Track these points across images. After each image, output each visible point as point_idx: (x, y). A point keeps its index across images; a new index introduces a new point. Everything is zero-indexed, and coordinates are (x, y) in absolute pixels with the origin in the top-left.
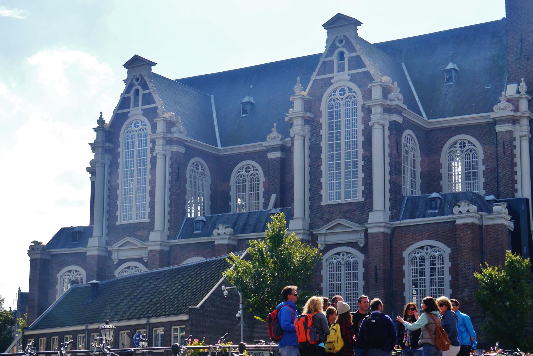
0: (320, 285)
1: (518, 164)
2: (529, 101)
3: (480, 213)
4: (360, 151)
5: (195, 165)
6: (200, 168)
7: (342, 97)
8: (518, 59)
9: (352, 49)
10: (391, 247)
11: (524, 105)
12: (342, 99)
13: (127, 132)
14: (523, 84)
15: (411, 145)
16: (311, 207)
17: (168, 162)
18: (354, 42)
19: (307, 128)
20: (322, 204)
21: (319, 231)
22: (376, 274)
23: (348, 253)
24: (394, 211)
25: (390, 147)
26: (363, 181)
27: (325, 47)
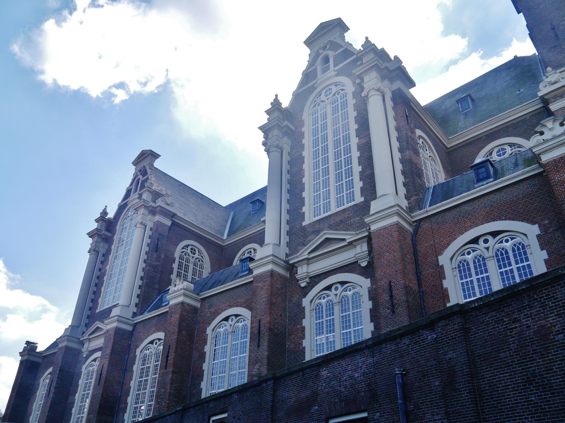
0: (301, 344)
5: (190, 248)
6: (197, 253)
7: (327, 97)
10: (415, 253)
13: (125, 219)
17: (148, 232)
19: (285, 139)
20: (304, 224)
21: (297, 257)
22: (391, 296)
23: (343, 283)
25: (396, 119)
26: (360, 175)
27: (308, 61)
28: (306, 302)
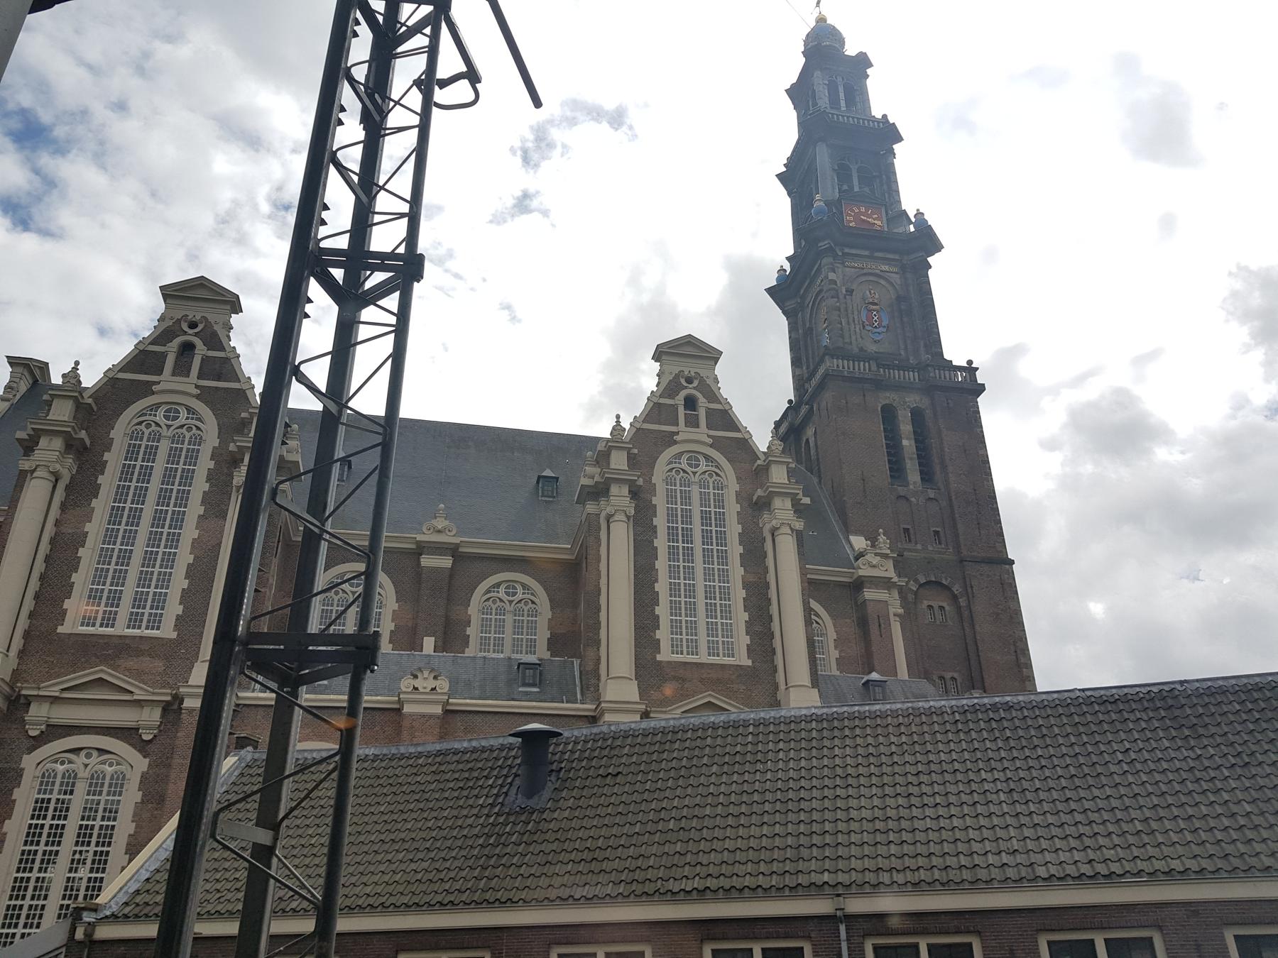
12: (694, 473)
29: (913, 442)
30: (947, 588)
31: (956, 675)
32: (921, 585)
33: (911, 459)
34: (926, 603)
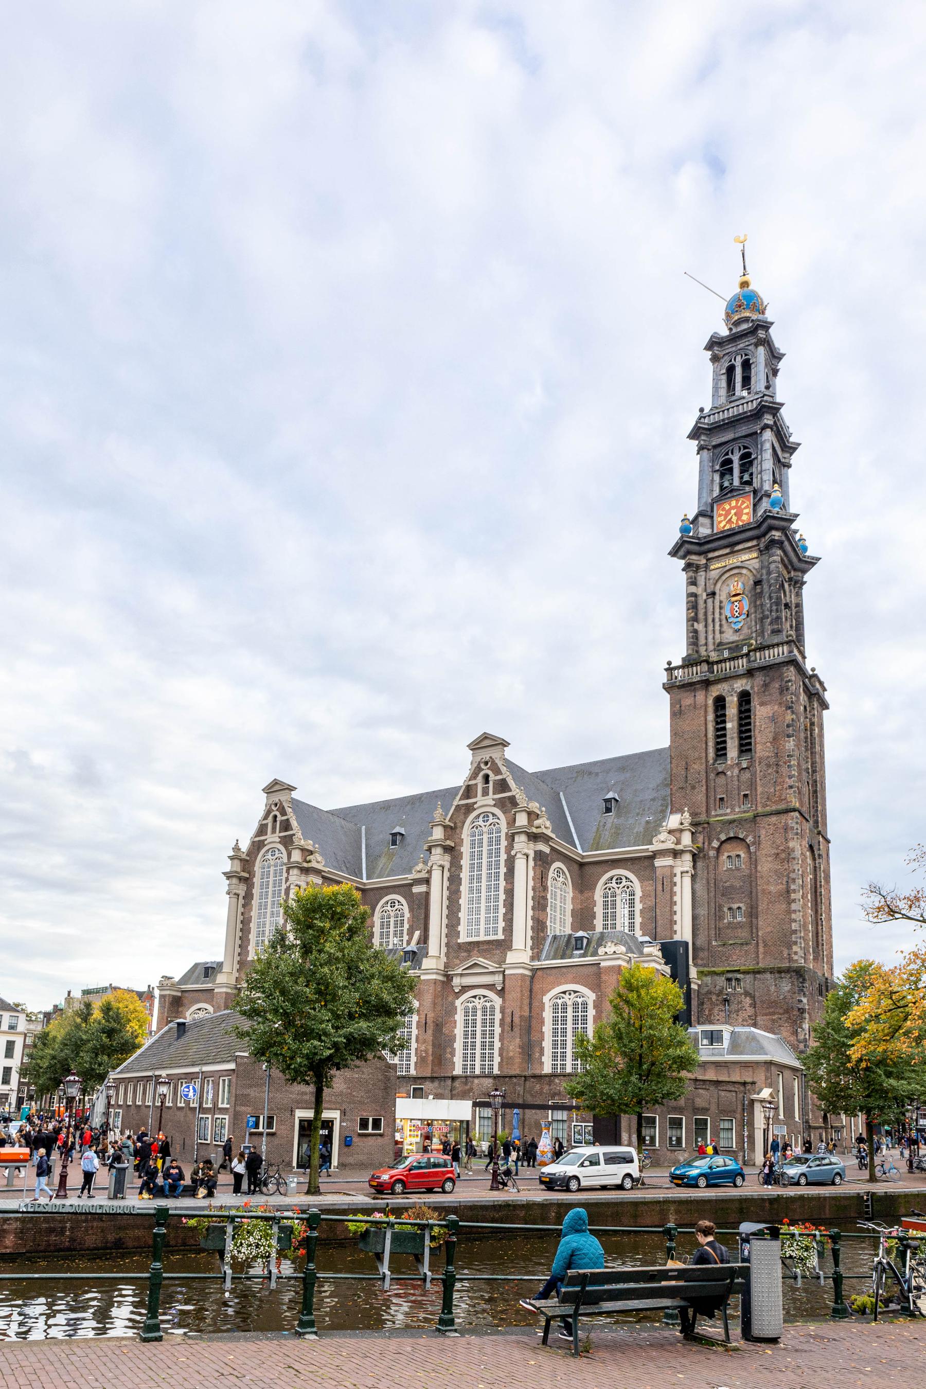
1: (679, 903)
2: (693, 833)
3: (629, 955)
4: (502, 883)
8: (682, 788)
9: (497, 771)
11: (686, 839)
14: (686, 815)
15: (561, 879)
16: (447, 945)
18: (500, 763)
19: (447, 857)
24: (536, 950)
28: (458, 1003)
29: (735, 724)
30: (743, 840)
31: (741, 905)
32: (722, 843)
33: (732, 738)
34: (726, 854)
